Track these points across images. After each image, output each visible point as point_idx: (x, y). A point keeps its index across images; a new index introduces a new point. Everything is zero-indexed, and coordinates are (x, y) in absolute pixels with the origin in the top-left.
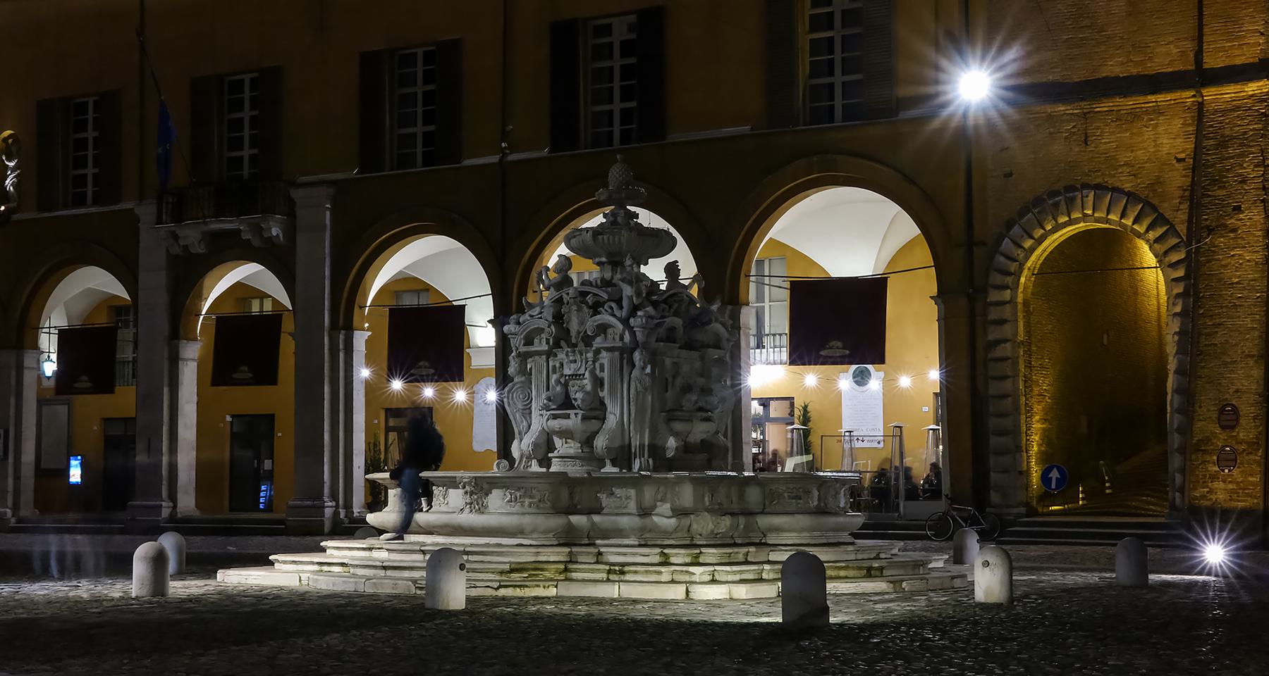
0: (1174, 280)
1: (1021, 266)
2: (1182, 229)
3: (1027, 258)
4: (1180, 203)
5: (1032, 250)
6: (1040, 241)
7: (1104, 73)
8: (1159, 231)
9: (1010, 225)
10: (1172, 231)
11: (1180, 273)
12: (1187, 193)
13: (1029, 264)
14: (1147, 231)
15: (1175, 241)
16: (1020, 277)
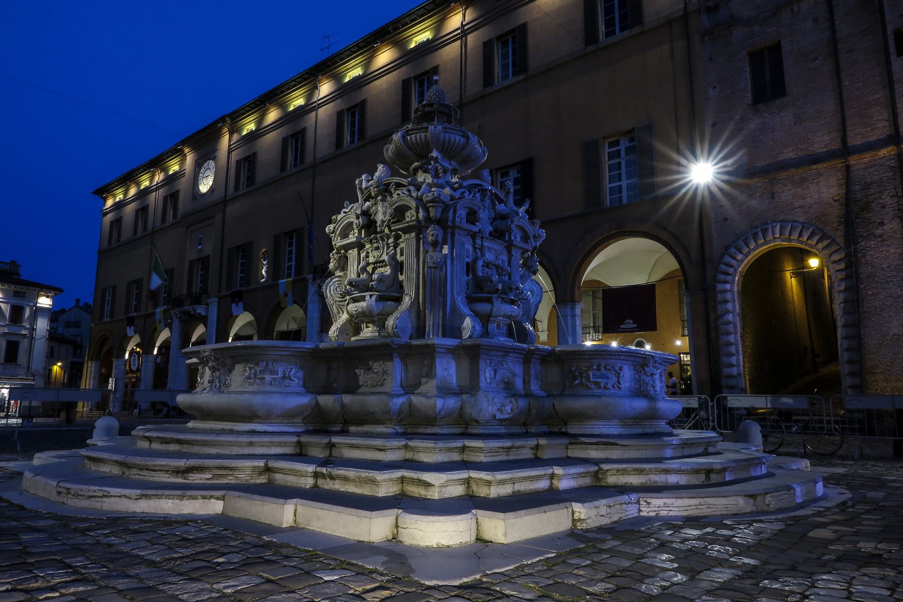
0: (838, 271)
1: (736, 270)
2: (840, 241)
3: (739, 266)
4: (838, 226)
5: (742, 261)
6: (747, 256)
7: (782, 157)
8: (825, 243)
9: (727, 248)
10: (833, 241)
11: (842, 266)
12: (843, 219)
13: (740, 269)
14: (817, 243)
15: (835, 248)
16: (735, 277)
